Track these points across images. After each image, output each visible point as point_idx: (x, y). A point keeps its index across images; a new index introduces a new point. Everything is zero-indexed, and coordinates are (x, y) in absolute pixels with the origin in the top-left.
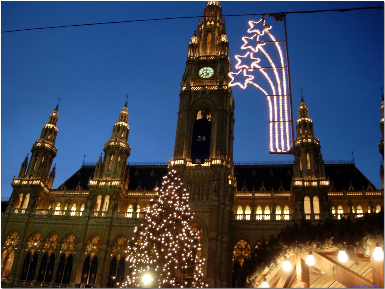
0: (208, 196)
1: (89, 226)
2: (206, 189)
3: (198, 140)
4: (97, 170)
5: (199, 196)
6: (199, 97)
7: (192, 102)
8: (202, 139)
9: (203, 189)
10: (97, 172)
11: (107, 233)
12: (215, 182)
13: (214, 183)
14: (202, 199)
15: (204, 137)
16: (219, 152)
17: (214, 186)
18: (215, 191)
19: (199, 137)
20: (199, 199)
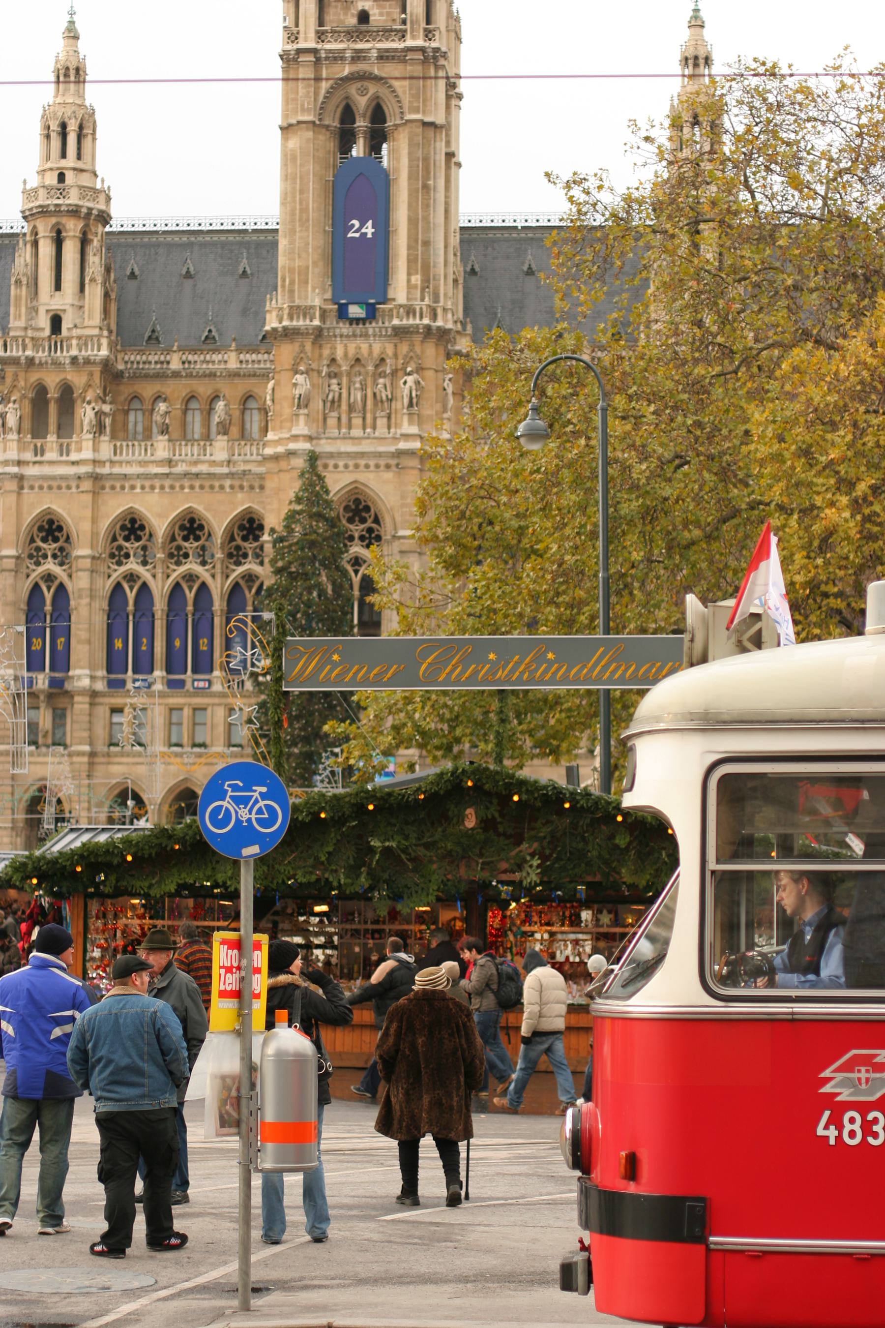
0: (389, 418)
1: (26, 491)
2: (384, 398)
3: (350, 235)
4: (18, 298)
5: (364, 419)
6: (346, 72)
7: (323, 92)
8: (363, 230)
9: (375, 394)
10: (18, 305)
11: (88, 513)
12: (410, 379)
13: (405, 383)
14: (374, 427)
15: (370, 223)
16: (417, 279)
17: (406, 392)
18: (411, 404)
19: (353, 225)
20: (364, 427)
